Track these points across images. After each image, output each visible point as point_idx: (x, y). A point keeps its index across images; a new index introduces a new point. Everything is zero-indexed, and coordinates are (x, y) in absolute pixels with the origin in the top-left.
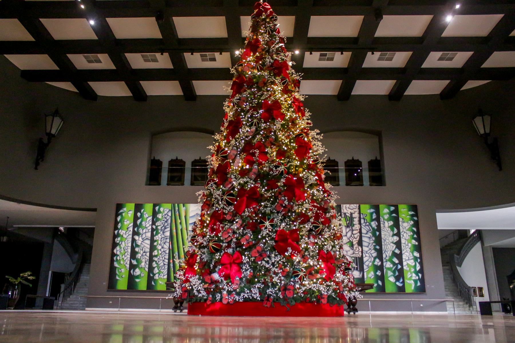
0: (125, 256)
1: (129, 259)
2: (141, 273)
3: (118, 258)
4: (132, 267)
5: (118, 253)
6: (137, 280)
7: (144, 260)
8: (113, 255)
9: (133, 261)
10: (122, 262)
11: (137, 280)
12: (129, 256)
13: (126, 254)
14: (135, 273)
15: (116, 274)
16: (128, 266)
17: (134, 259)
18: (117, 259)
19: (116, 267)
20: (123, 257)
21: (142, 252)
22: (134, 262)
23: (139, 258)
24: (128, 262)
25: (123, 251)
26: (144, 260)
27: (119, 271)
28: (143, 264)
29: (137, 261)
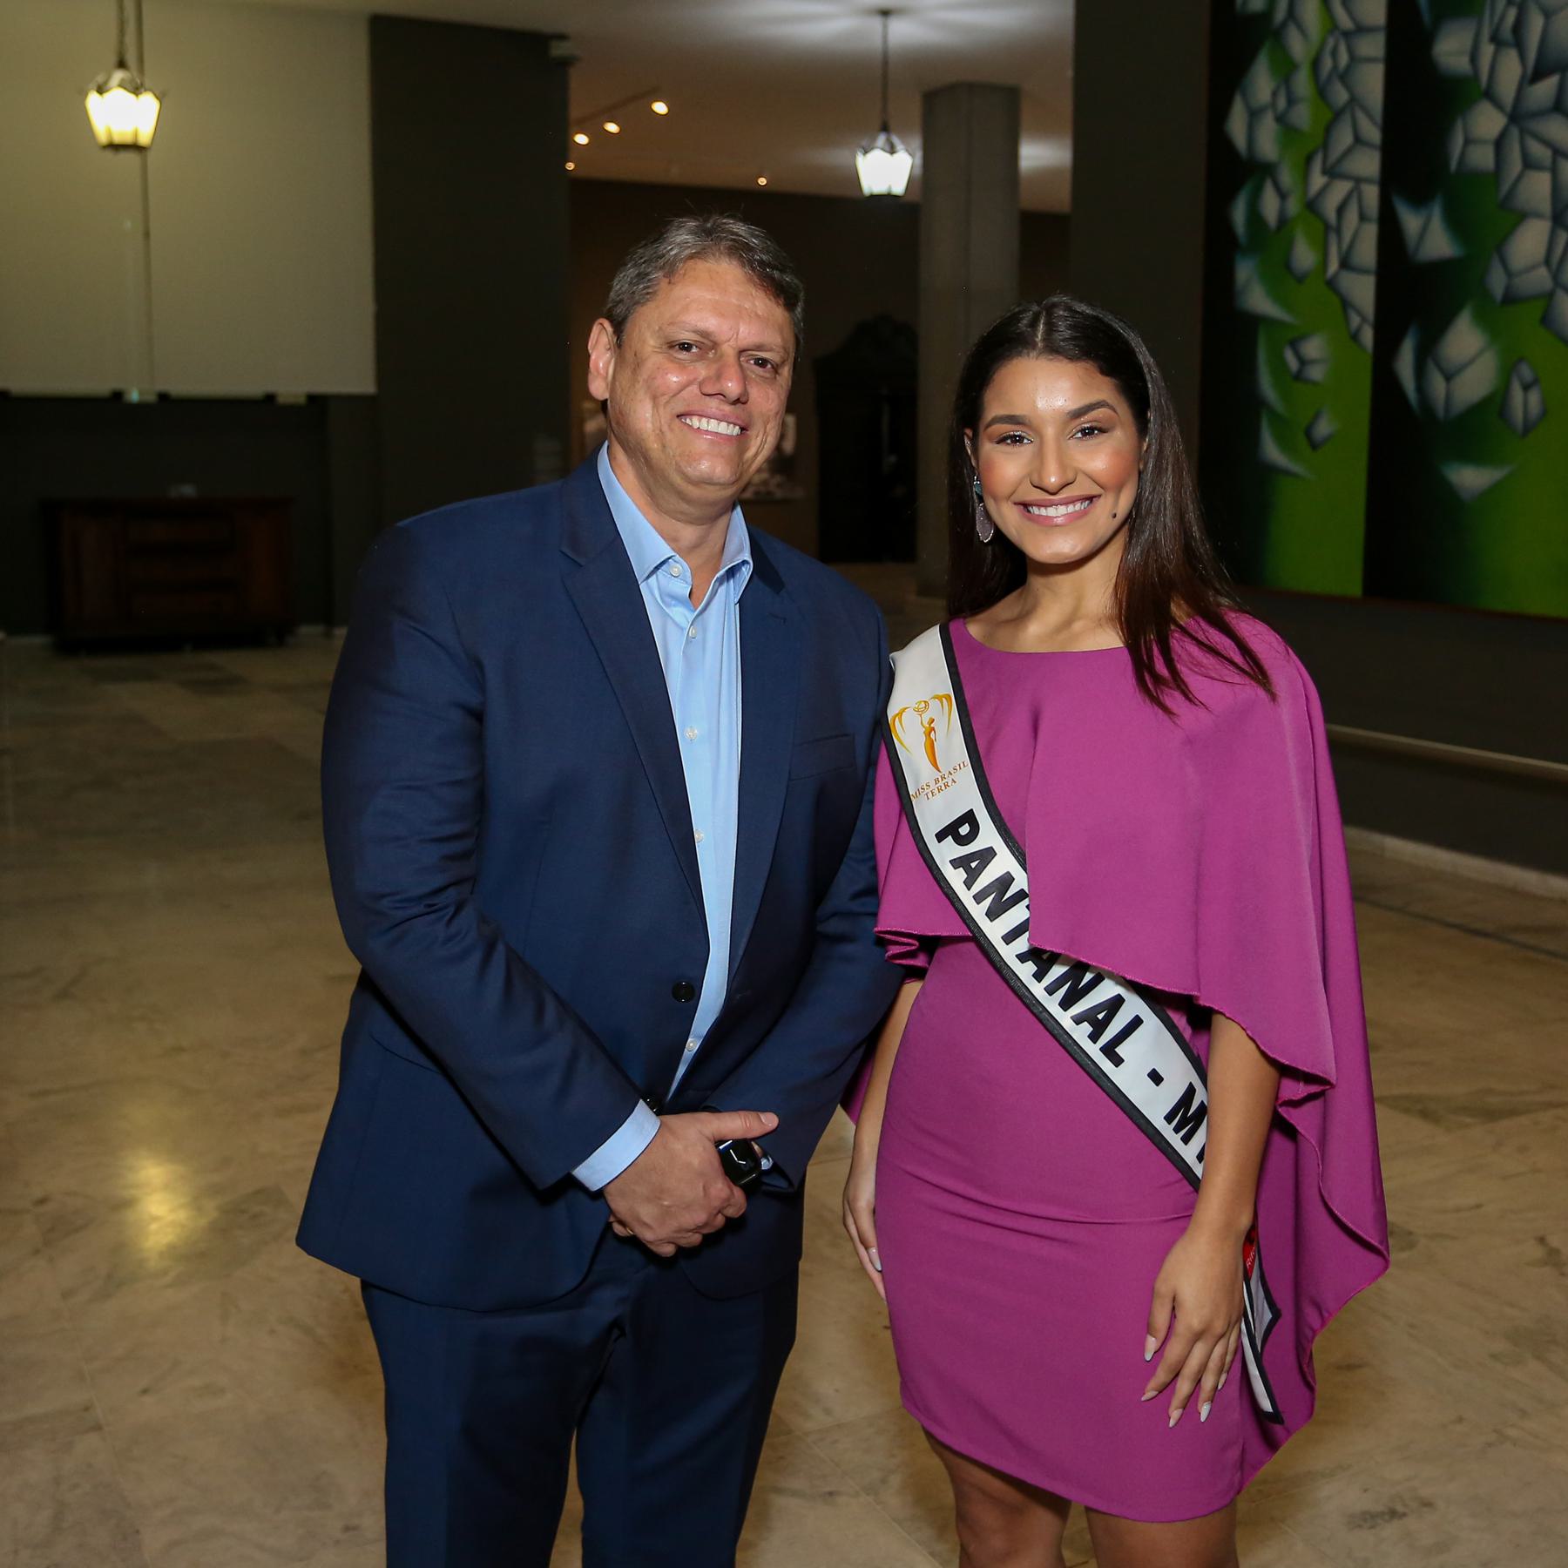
0: (1332, 173)
1: (1372, 194)
2: (1508, 370)
3: (1270, 206)
4: (1414, 300)
5: (1268, 145)
6: (1469, 478)
7: (1537, 189)
8: (1232, 171)
9: (1411, 221)
10: (1304, 255)
11: (1469, 478)
12: (1368, 164)
13: (1344, 138)
14: (1438, 385)
15: (1254, 405)
16: (1363, 291)
17: (1419, 200)
18: (1255, 216)
19: (1252, 323)
20: (1318, 180)
21: (1510, 71)
22: (1431, 236)
23: (1483, 158)
24: (1367, 251)
25: (1303, 116)
26: (1537, 189)
27: (1279, 365)
28: (1530, 243)
29: (1457, 224)
